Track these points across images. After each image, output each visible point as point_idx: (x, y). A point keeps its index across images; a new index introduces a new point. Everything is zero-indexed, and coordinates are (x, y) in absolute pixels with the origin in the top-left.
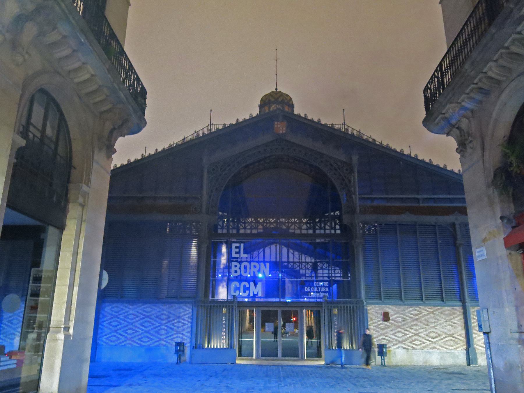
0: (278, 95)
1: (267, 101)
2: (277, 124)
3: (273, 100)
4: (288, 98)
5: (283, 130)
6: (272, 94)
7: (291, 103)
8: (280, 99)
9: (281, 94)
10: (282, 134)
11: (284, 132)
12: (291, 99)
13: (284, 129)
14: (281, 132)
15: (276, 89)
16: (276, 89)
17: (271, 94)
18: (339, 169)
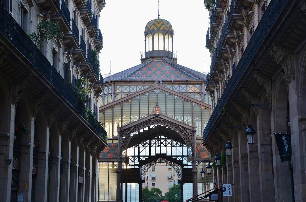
0: (160, 25)
1: (151, 30)
2: (155, 109)
3: (156, 29)
4: (168, 26)
5: (158, 112)
6: (155, 23)
7: (170, 30)
8: (161, 29)
9: (162, 20)
10: (158, 114)
11: (159, 113)
12: (171, 27)
13: (159, 111)
14: (157, 113)
15: (159, 15)
16: (159, 15)
17: (155, 20)
18: (187, 133)
